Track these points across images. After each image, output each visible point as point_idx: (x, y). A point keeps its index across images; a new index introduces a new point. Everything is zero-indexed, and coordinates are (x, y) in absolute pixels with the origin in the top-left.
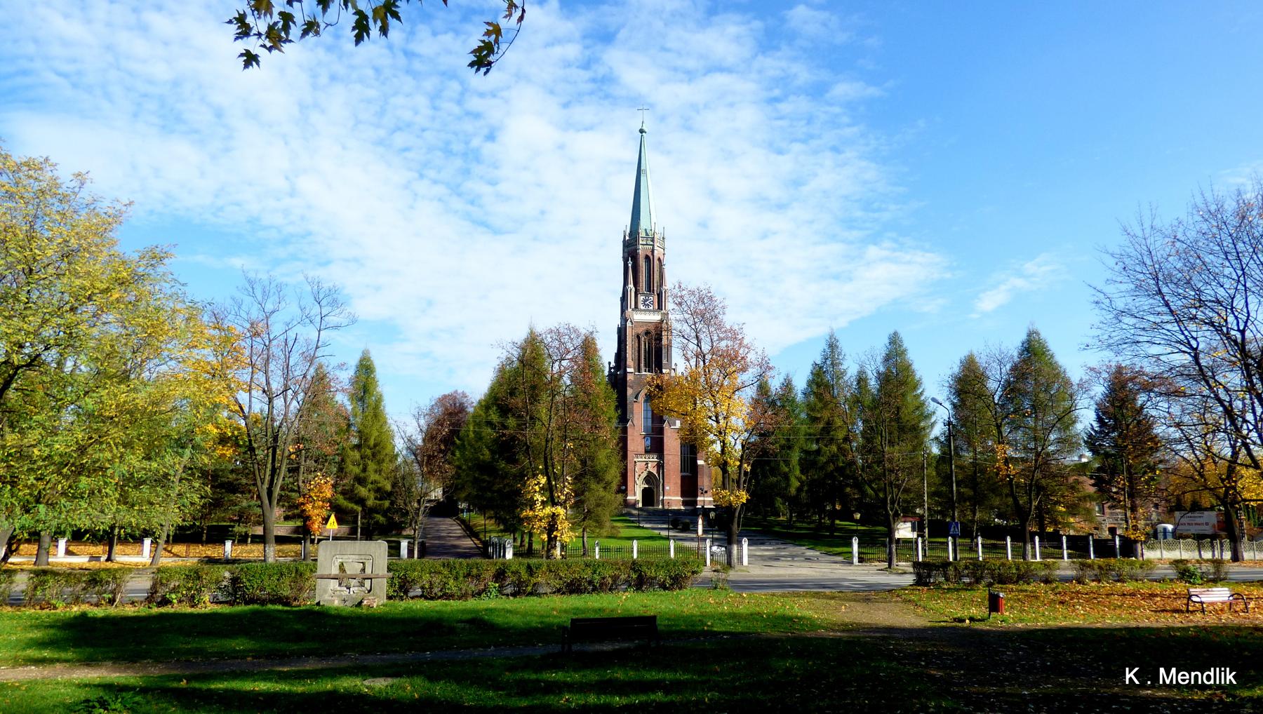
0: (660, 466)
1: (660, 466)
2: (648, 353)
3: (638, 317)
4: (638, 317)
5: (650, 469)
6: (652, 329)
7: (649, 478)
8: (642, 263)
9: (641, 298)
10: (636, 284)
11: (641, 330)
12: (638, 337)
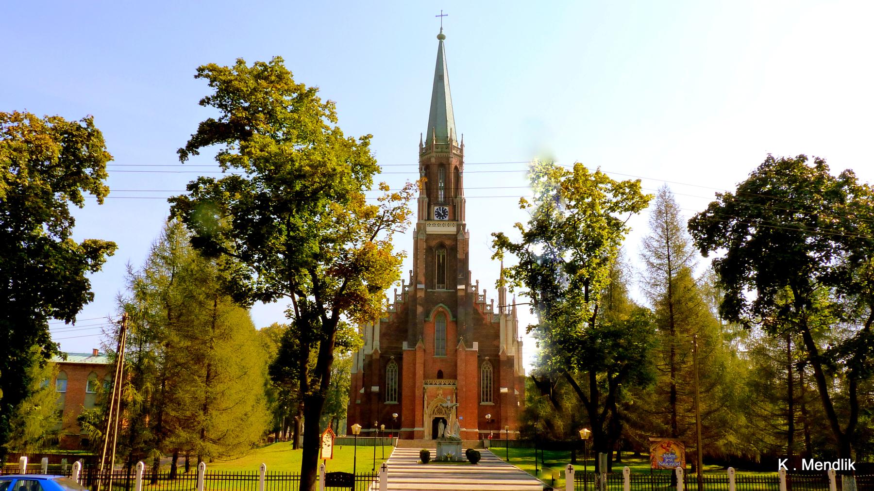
3: (432, 229)
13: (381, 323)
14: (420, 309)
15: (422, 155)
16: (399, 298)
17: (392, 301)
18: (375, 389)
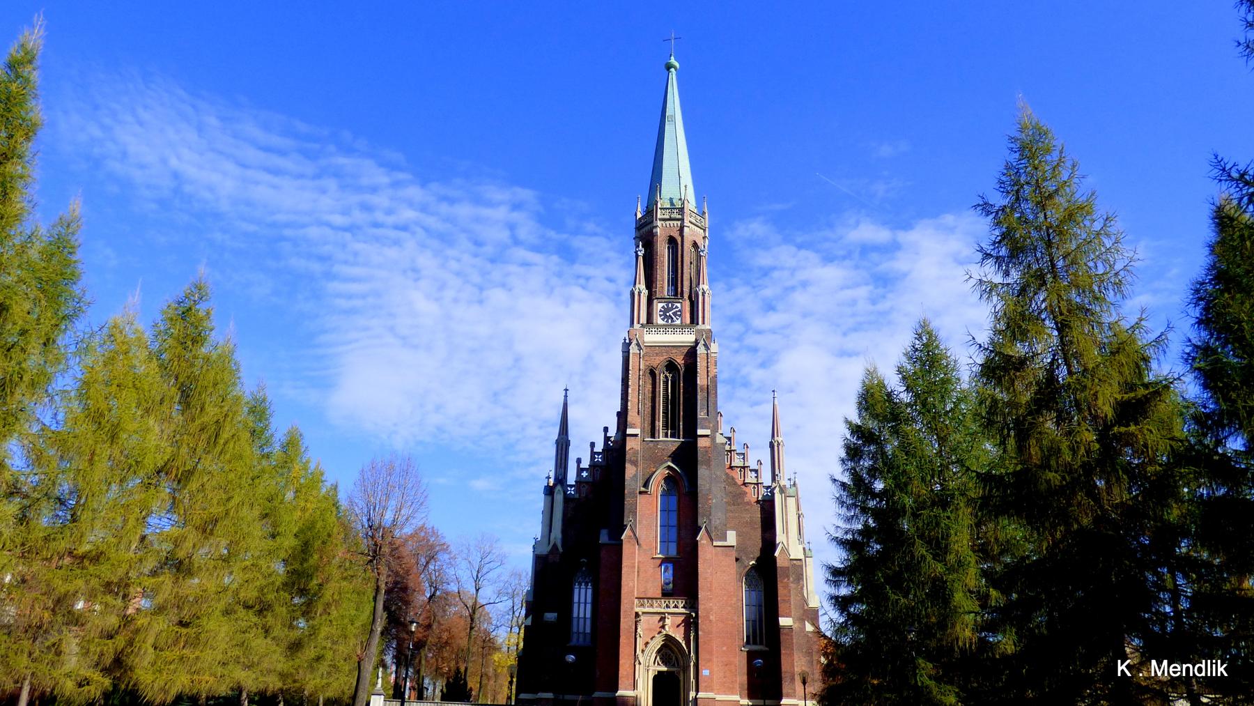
0: (691, 624)
1: (691, 624)
2: (671, 403)
3: (651, 338)
4: (651, 338)
5: (669, 630)
6: (680, 360)
7: (669, 651)
8: (663, 250)
9: (659, 306)
10: (650, 283)
11: (658, 361)
12: (652, 373)
13: (567, 499)
14: (630, 471)
15: (638, 228)
16: (599, 459)
17: (585, 464)
18: (551, 616)
